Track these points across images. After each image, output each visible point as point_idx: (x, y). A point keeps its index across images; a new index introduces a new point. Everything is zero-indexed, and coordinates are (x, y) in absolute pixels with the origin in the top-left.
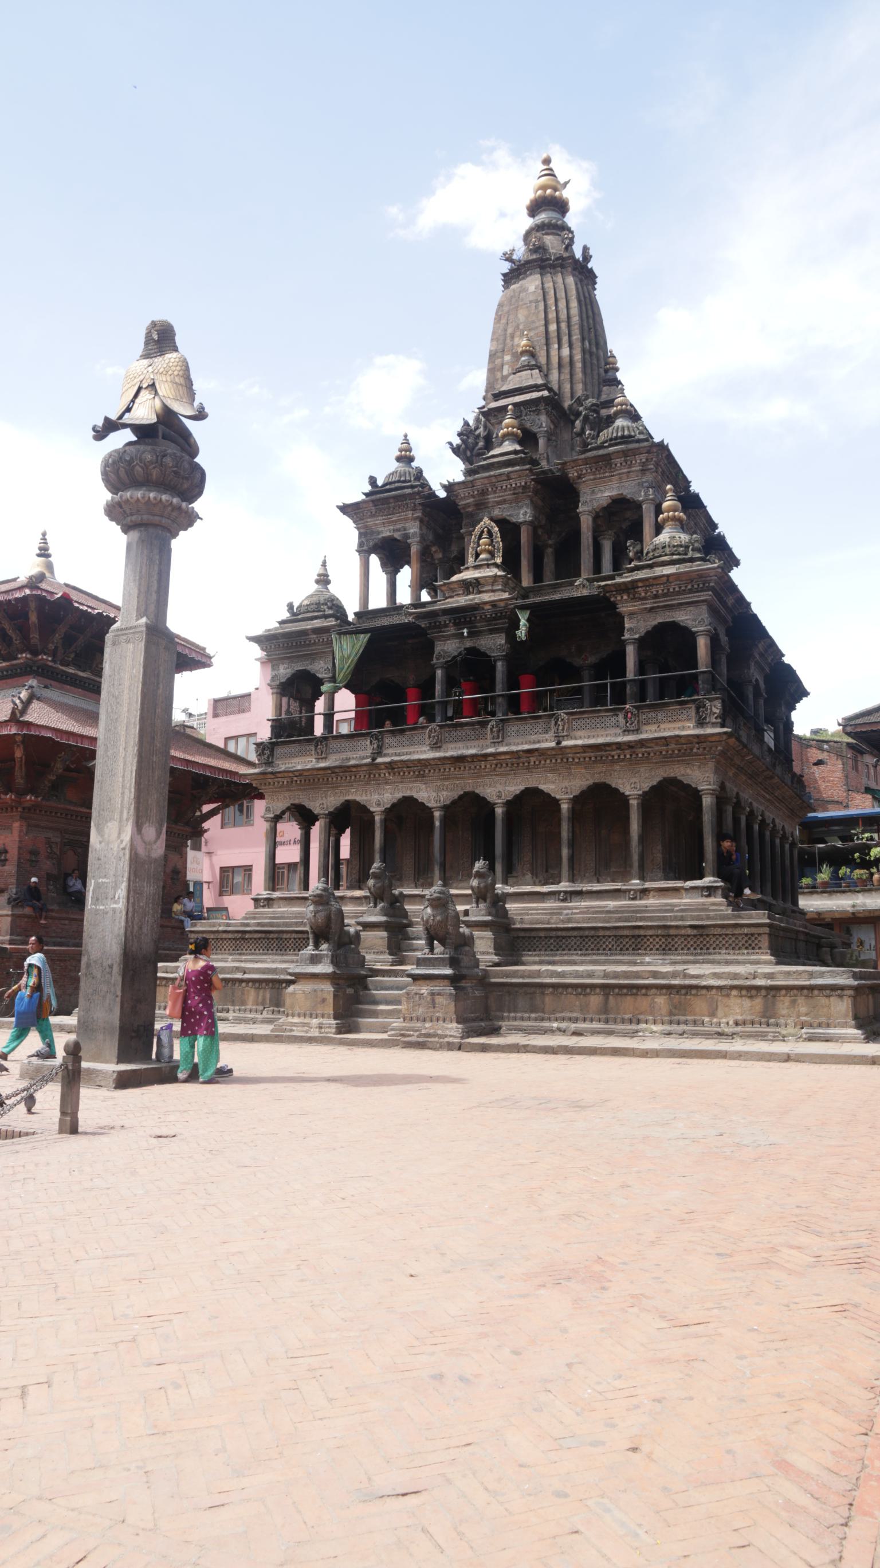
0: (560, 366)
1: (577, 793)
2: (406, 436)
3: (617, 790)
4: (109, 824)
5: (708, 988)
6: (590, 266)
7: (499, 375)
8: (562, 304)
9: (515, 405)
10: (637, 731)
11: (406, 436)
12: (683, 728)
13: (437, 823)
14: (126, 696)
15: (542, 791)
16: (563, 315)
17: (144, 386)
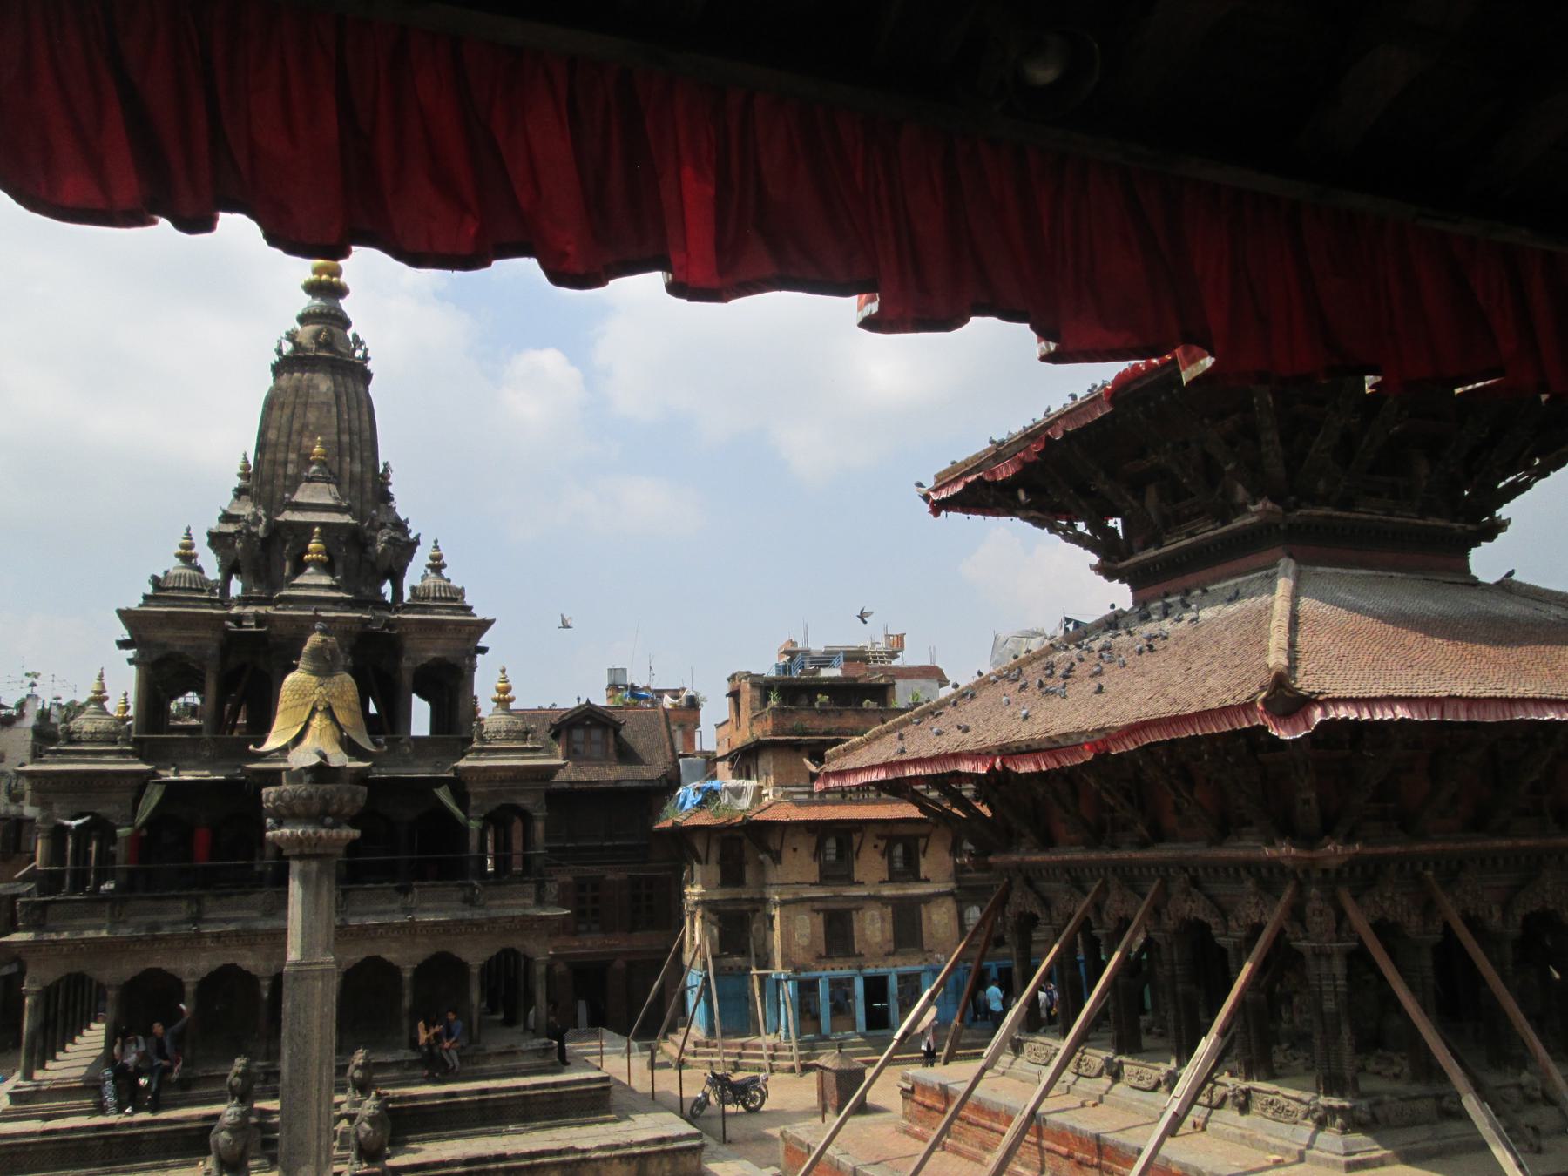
0: (352, 482)
1: (420, 961)
2: (188, 529)
3: (459, 959)
4: (304, 1169)
5: (596, 1160)
6: (369, 366)
7: (280, 471)
8: (354, 415)
9: (323, 525)
10: (482, 906)
11: (188, 529)
12: (525, 906)
13: (266, 994)
14: (316, 1034)
15: (384, 960)
16: (356, 424)
17: (320, 708)
